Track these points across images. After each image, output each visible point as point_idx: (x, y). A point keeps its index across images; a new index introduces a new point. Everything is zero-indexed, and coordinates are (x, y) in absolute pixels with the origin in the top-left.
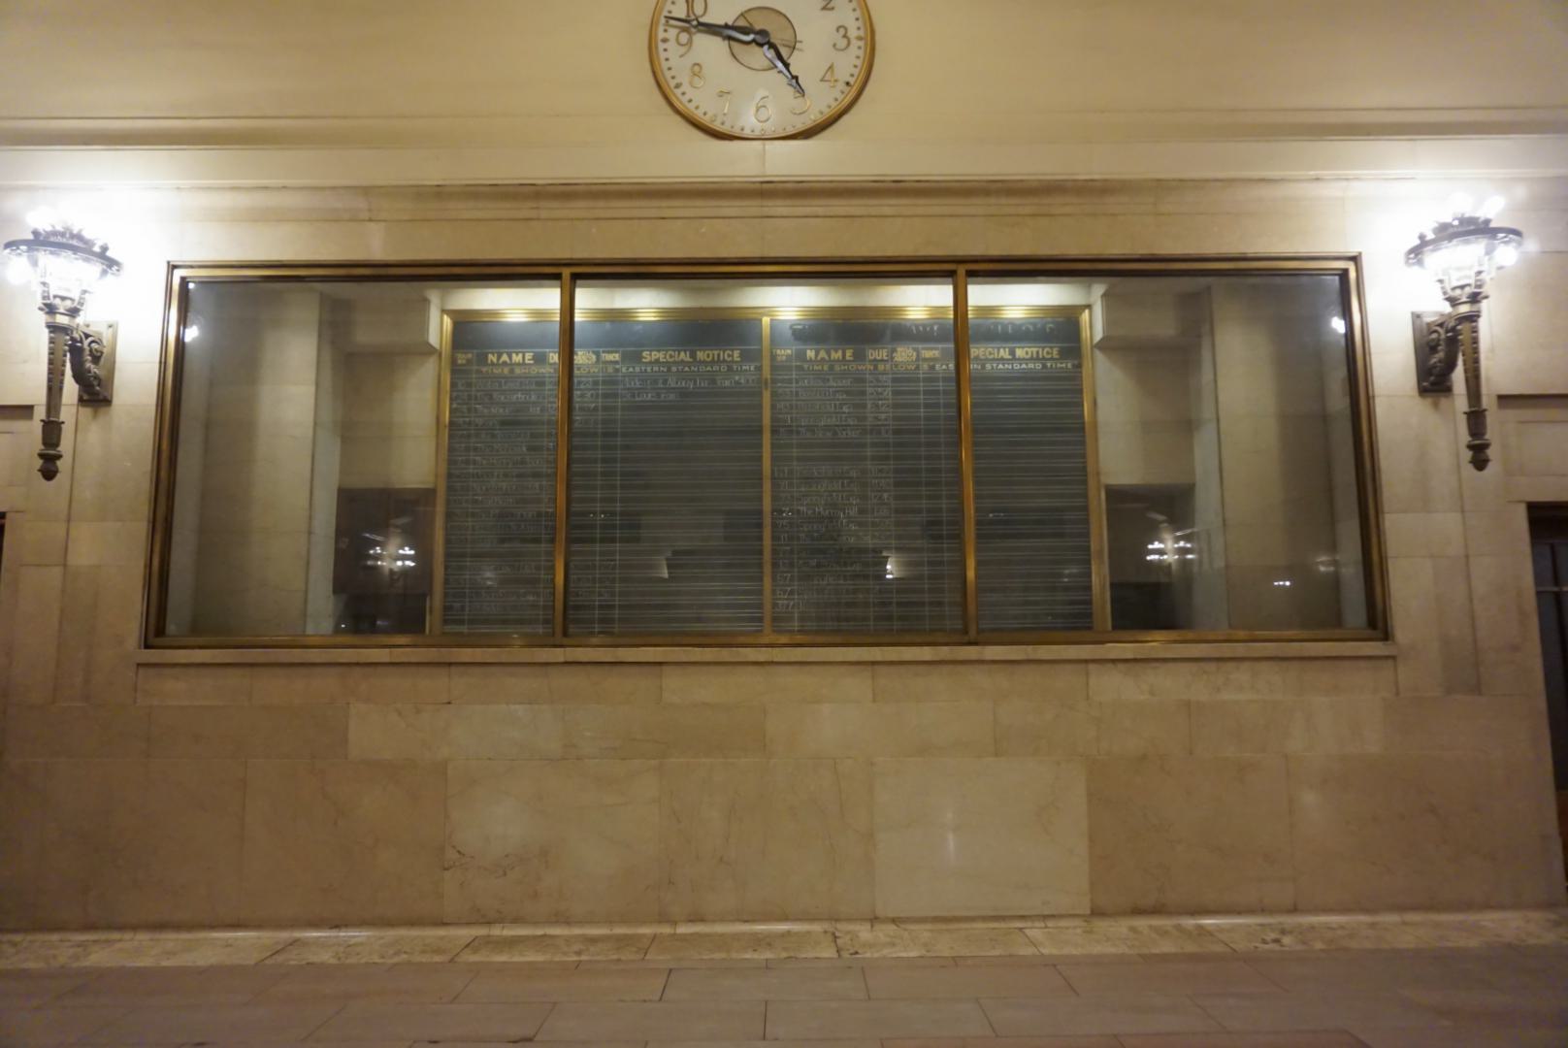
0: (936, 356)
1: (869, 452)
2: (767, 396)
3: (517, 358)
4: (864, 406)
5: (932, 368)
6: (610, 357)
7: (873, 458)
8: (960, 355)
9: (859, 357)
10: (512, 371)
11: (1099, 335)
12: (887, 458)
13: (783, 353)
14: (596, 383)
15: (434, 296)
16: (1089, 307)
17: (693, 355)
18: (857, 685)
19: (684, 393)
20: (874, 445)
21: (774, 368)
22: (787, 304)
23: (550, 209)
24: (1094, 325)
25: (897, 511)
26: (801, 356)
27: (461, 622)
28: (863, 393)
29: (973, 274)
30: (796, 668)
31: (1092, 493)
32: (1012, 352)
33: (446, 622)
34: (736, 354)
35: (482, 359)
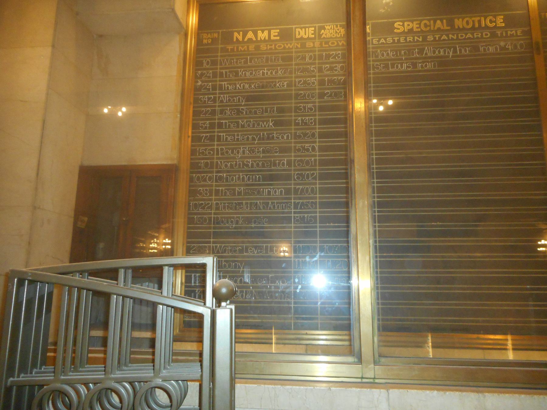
3: (262, 35)
10: (257, 48)
17: (451, 23)
35: (228, 38)
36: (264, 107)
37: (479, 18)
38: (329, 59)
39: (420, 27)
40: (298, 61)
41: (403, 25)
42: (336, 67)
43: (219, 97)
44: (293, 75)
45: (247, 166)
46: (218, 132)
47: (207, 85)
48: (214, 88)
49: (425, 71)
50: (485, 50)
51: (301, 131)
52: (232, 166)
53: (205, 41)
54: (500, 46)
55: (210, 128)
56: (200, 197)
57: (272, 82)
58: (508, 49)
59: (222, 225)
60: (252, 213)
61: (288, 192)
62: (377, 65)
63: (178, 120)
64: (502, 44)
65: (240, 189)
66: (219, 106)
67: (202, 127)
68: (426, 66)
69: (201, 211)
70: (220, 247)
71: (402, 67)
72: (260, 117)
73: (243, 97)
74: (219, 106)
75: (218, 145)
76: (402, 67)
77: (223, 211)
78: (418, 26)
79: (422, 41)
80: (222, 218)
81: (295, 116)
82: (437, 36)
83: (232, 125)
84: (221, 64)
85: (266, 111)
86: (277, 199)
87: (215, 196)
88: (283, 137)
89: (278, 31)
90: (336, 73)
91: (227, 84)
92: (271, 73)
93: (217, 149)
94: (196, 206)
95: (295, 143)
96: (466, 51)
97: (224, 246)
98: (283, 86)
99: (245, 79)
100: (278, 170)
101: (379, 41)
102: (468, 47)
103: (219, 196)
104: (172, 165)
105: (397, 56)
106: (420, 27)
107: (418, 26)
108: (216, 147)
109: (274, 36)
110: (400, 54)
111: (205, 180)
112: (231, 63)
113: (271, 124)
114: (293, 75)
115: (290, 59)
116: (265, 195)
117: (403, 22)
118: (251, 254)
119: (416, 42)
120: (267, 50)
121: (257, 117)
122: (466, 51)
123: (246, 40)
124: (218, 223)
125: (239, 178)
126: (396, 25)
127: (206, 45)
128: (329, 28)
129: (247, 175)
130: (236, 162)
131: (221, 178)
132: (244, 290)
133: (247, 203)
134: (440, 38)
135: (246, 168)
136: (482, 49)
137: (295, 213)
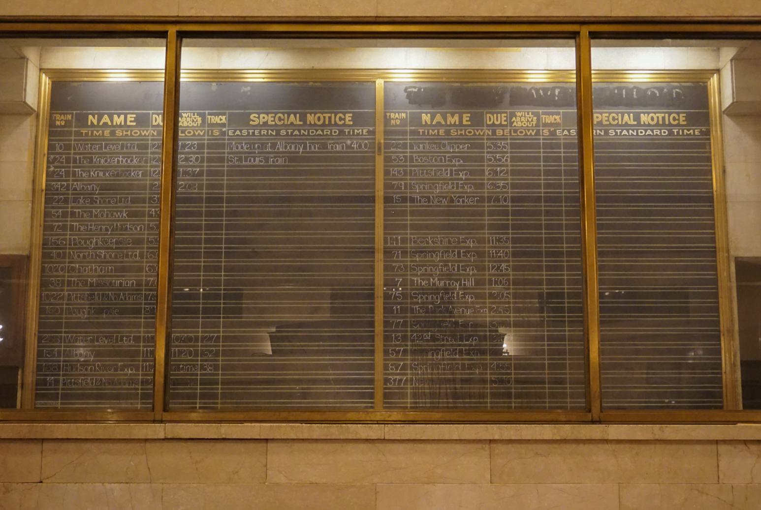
0: (558, 122)
1: (487, 220)
3: (118, 120)
5: (553, 133)
6: (216, 120)
7: (492, 227)
8: (583, 121)
9: (477, 121)
10: (113, 133)
11: (728, 101)
12: (506, 227)
13: (398, 117)
14: (201, 146)
15: (32, 53)
16: (718, 71)
17: (303, 118)
18: (473, 464)
19: (293, 158)
20: (491, 213)
21: (386, 133)
22: (402, 65)
24: (724, 90)
25: (516, 283)
26: (416, 120)
27: (55, 397)
28: (482, 159)
29: (594, 35)
30: (408, 446)
32: (637, 118)
33: (38, 396)
34: (348, 117)
35: (82, 120)
36: (118, 196)
37: (329, 115)
38: (185, 149)
39: (274, 121)
40: (153, 150)
41: (259, 118)
42: (191, 157)
43: (73, 185)
44: (149, 165)
45: (100, 257)
46: (71, 221)
47: (61, 171)
48: (67, 174)
49: (275, 166)
50: (332, 147)
51: (154, 223)
52: (84, 257)
53: (58, 123)
54: (346, 145)
55: (62, 217)
56: (52, 287)
57: (127, 171)
58: (353, 148)
59: (74, 316)
60: (103, 304)
62: (231, 157)
63: (30, 208)
64: (349, 142)
65: (92, 280)
66: (73, 194)
67: (54, 215)
68: (277, 161)
69: (52, 301)
70: (72, 337)
71: (254, 161)
72: (113, 207)
73: (97, 185)
74: (73, 194)
75: (70, 235)
76: (254, 161)
77: (75, 302)
78: (273, 119)
79: (276, 135)
80: (73, 308)
81: (149, 207)
82: (290, 131)
83: (85, 215)
84: (75, 149)
85: (121, 202)
86: (129, 290)
87: (68, 286)
88: (136, 229)
89: (135, 116)
90: (191, 163)
91: (81, 171)
92: (127, 161)
93: (70, 239)
94: (48, 296)
95: (148, 234)
96: (315, 148)
97: (76, 336)
98: (138, 175)
99: (98, 167)
100: (129, 262)
101: (234, 133)
102: (317, 143)
103: (71, 287)
104: (22, 257)
105: (251, 149)
106: (274, 121)
107: (273, 119)
108: (68, 237)
109: (131, 121)
110: (254, 147)
111: (57, 271)
112: (85, 148)
113: (125, 215)
114: (149, 165)
115: (146, 147)
117: (259, 114)
118: (102, 344)
119: (270, 136)
120: (122, 136)
121: (110, 207)
122: (315, 148)
123: (101, 124)
124: (70, 313)
125: (91, 270)
126: (252, 117)
127: (58, 127)
128: (187, 116)
129: (99, 266)
130: (89, 252)
131: (73, 269)
132: (95, 378)
133: (98, 295)
134: (292, 133)
135: (98, 259)
136: (329, 147)
137: (145, 304)
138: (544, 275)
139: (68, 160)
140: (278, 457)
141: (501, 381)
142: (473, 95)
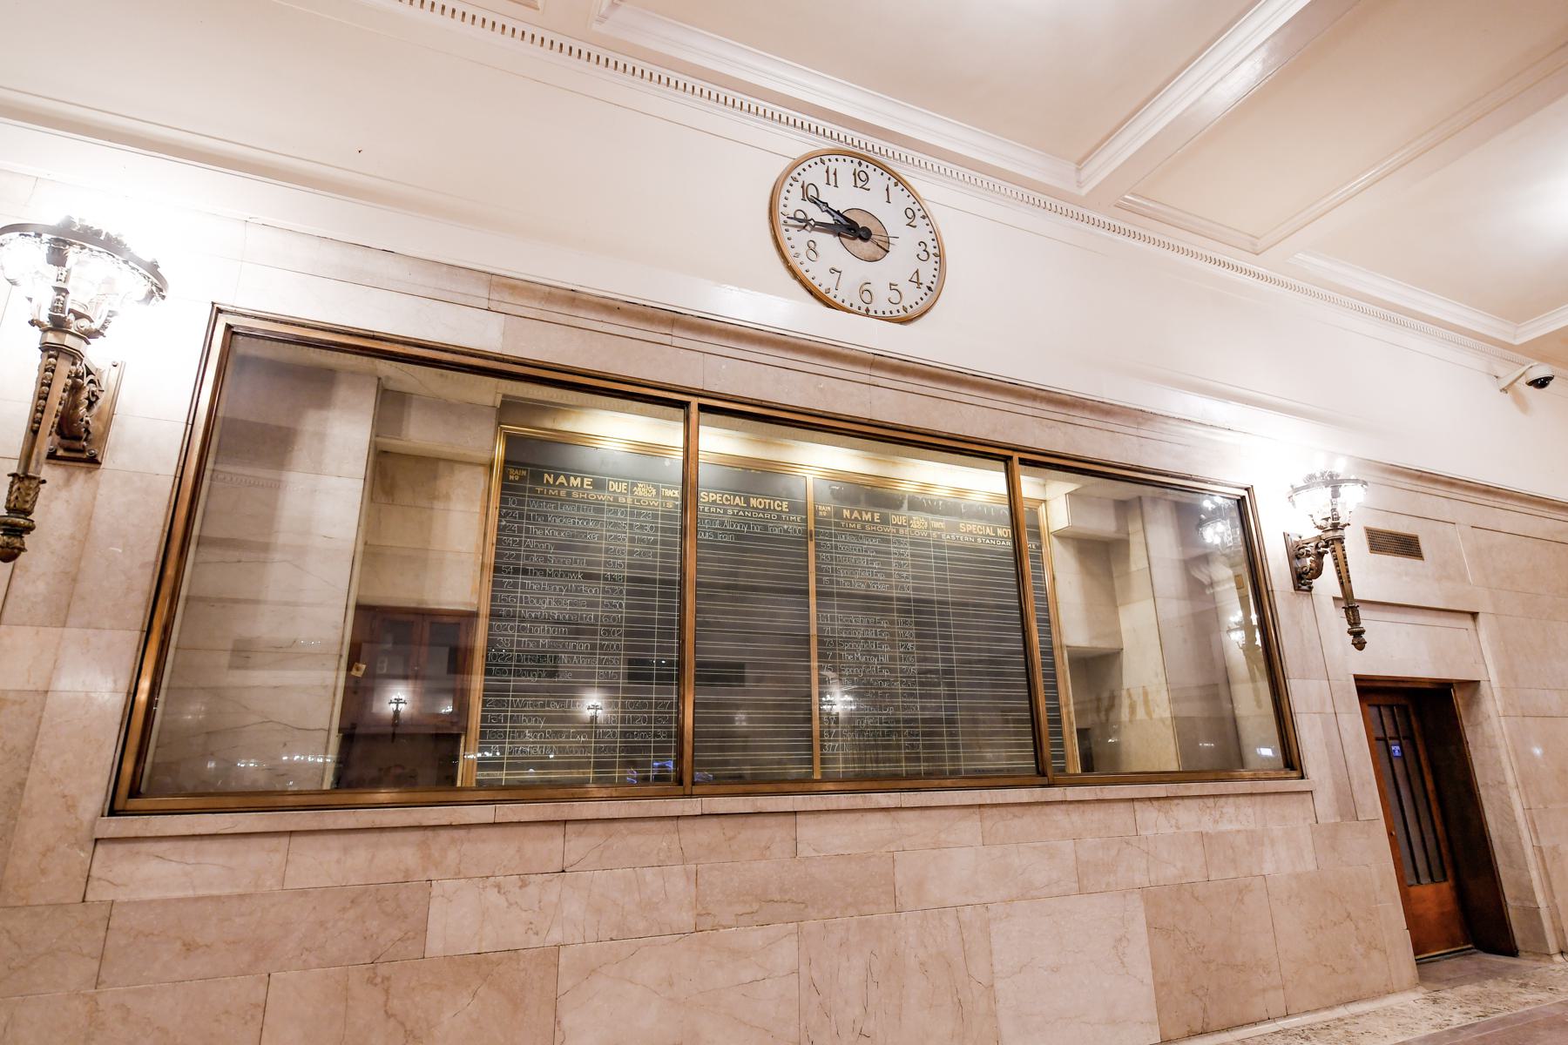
1: (895, 605)
2: (811, 545)
4: (890, 564)
7: (899, 611)
10: (569, 494)
12: (909, 611)
13: (825, 510)
17: (747, 501)
18: (969, 827)
19: (738, 537)
21: (816, 522)
23: (681, 338)
26: (838, 514)
30: (917, 813)
31: (1057, 653)
61: (594, 647)
116: (571, 649)
131: (524, 629)
138: (939, 654)
139: (521, 516)
140: (809, 830)
141: (913, 746)
142: (878, 496)
